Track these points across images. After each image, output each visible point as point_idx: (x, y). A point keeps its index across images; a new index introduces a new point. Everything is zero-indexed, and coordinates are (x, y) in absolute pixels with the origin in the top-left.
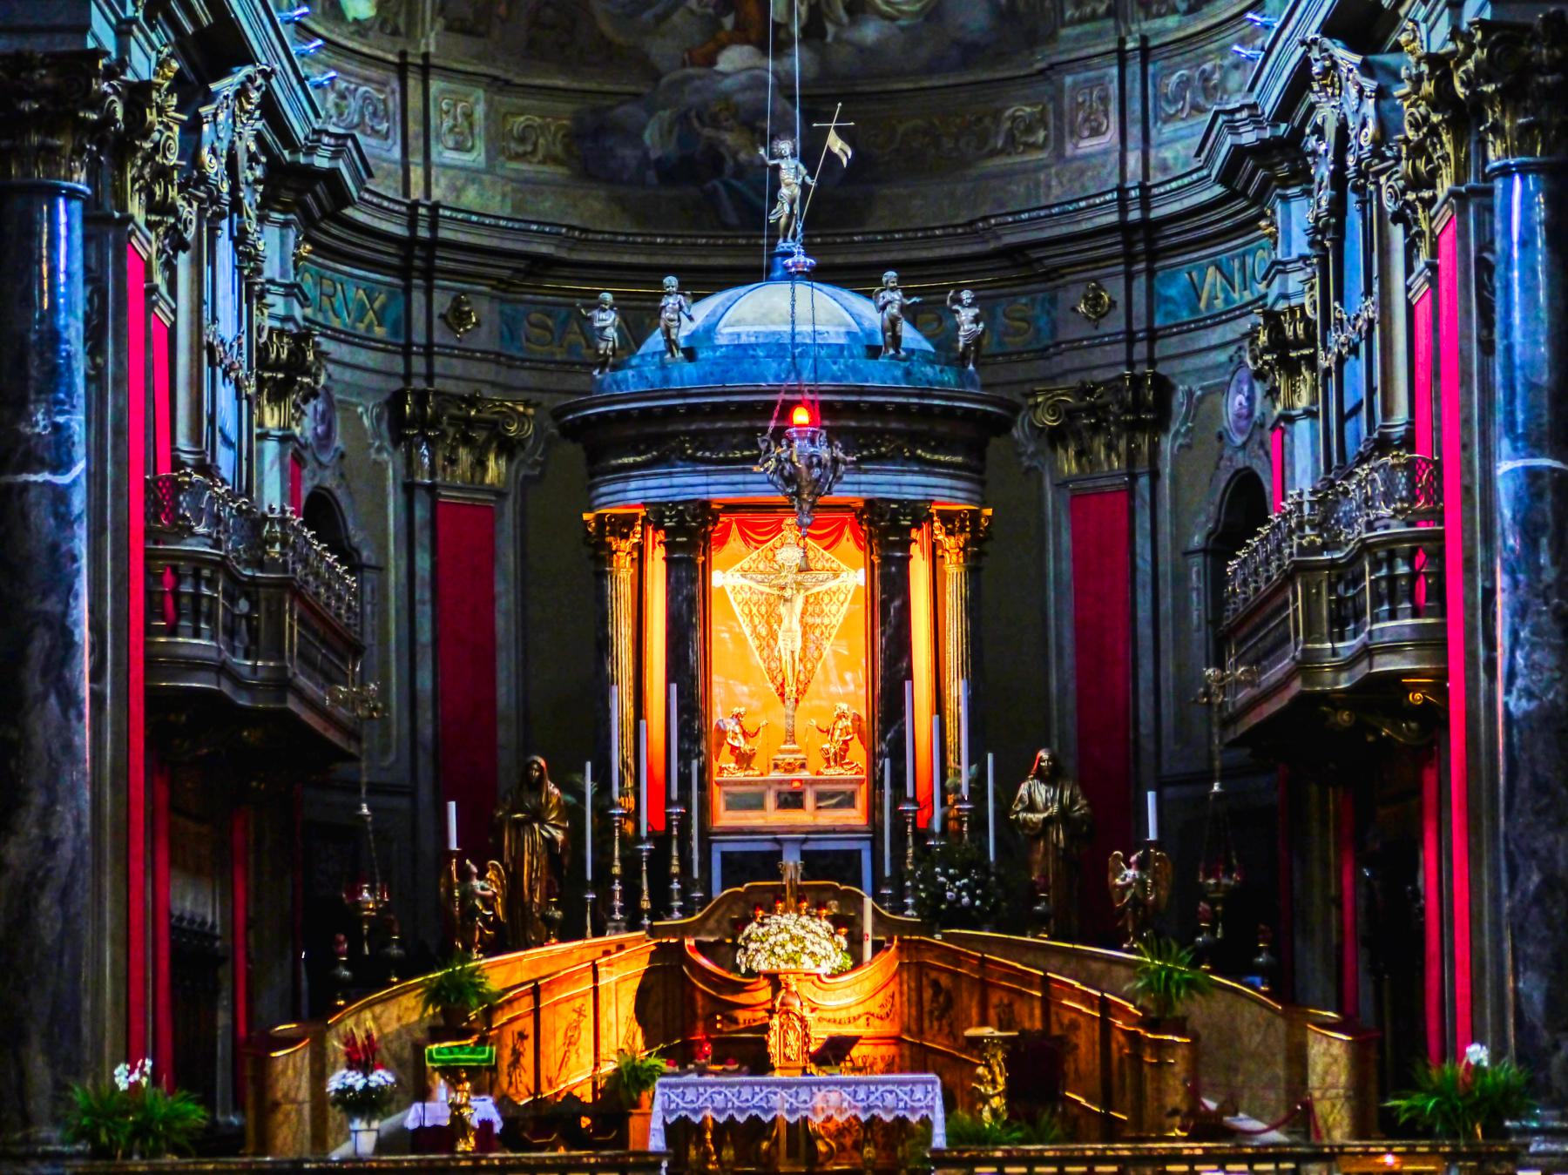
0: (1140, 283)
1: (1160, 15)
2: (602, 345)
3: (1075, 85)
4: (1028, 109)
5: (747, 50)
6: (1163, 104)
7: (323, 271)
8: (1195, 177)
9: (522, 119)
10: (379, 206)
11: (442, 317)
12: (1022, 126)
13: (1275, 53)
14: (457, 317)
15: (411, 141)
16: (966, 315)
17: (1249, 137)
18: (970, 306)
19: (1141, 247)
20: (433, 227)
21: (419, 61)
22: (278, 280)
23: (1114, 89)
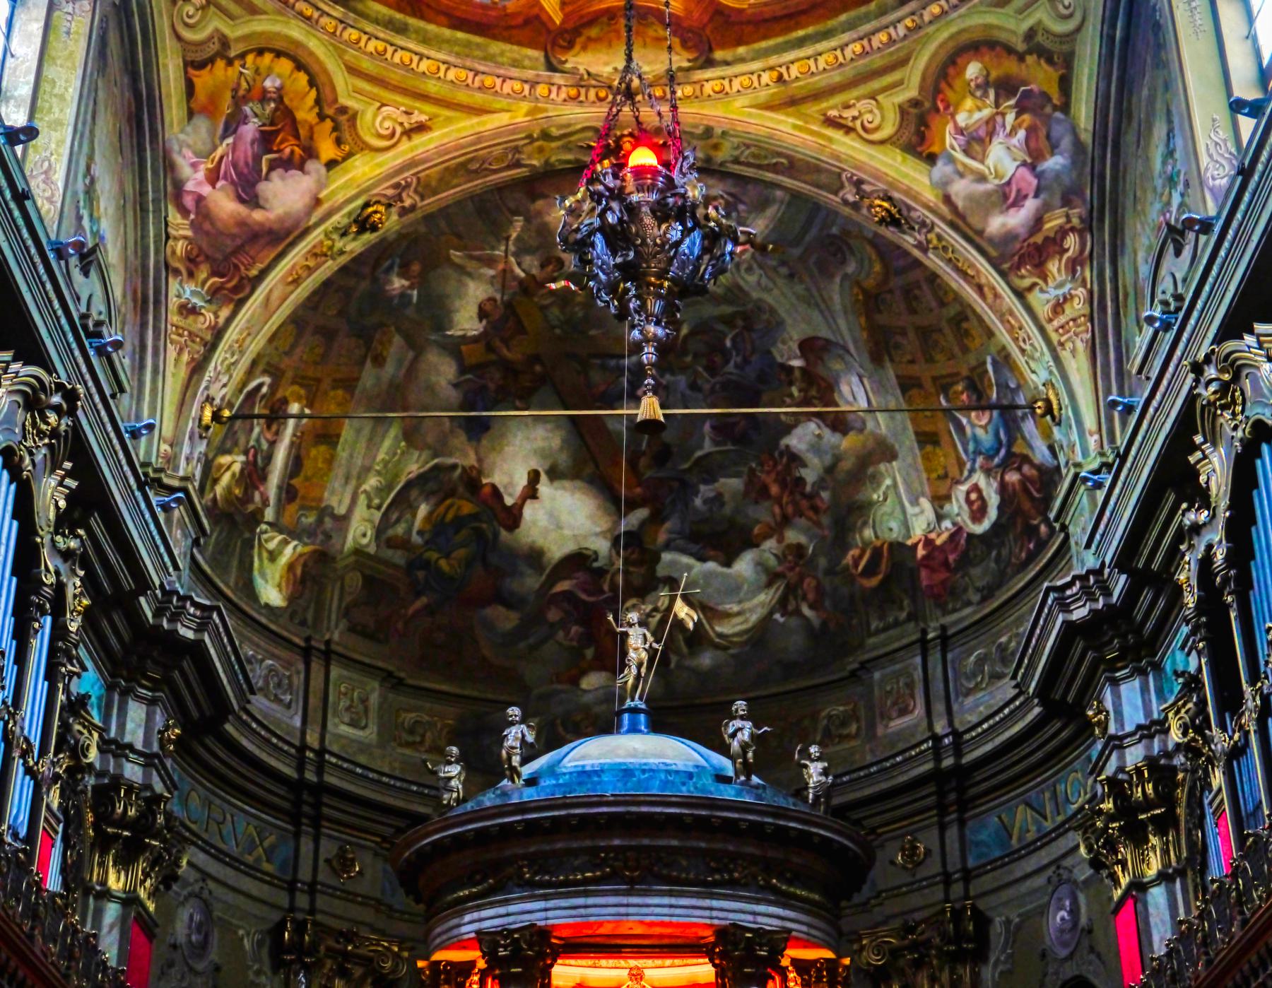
0: (952, 833)
1: (955, 610)
2: (446, 796)
3: (882, 680)
4: (841, 708)
6: (964, 682)
7: (212, 798)
8: (1006, 711)
9: (413, 715)
10: (268, 741)
11: (328, 861)
12: (837, 722)
13: (1130, 459)
14: (343, 863)
15: (310, 713)
18: (819, 759)
20: (320, 771)
21: (323, 647)
22: (139, 746)
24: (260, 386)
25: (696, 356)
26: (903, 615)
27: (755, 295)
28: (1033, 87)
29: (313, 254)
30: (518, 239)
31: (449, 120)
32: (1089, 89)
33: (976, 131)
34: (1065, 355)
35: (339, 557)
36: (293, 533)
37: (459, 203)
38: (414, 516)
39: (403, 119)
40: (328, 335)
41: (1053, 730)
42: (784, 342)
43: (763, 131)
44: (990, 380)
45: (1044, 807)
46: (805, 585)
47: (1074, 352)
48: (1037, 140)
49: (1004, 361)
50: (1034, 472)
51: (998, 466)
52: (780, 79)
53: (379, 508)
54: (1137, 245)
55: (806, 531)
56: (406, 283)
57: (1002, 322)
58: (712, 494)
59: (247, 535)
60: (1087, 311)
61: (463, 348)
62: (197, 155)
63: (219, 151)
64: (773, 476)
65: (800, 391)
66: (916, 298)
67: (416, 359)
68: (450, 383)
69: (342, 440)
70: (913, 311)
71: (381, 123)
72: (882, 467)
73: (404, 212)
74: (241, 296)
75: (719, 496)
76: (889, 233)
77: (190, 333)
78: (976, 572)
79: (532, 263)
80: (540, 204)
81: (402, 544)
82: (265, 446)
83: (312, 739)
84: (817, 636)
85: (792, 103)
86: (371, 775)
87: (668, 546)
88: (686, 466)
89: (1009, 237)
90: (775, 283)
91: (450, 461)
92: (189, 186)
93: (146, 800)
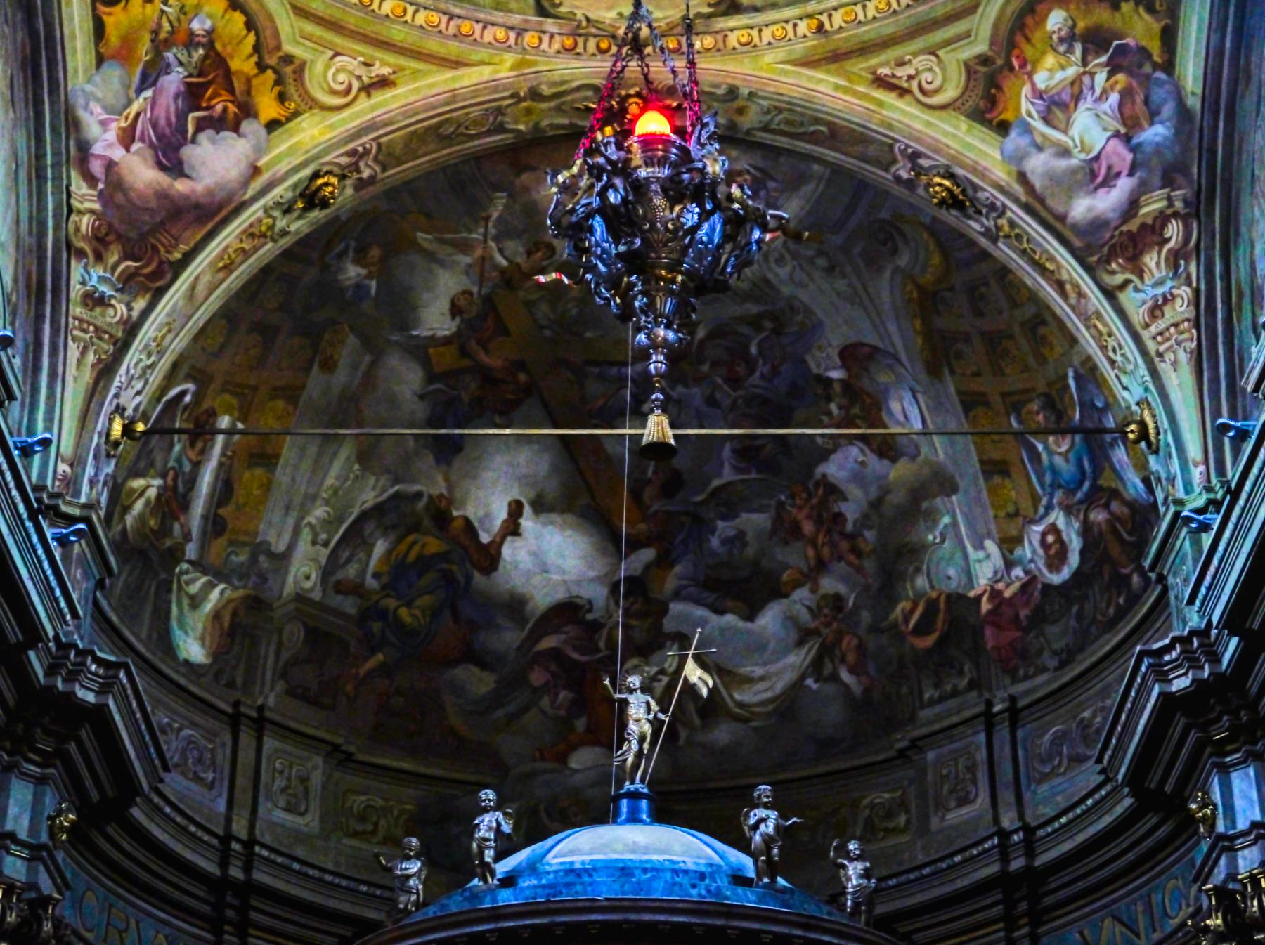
1: (1027, 677)
2: (403, 898)
4: (886, 796)
5: (597, 750)
6: (1037, 765)
7: (113, 898)
8: (1090, 802)
9: (363, 798)
10: (184, 829)
13: (1244, 496)
15: (238, 793)
16: (854, 870)
17: (1180, 683)
18: (859, 858)
19: (1023, 906)
20: (248, 868)
21: (254, 714)
22: (23, 835)
23: (982, 755)
24: (183, 394)
25: (714, 364)
26: (963, 683)
27: (786, 290)
28: (1129, 41)
29: (250, 234)
30: (500, 218)
31: (416, 74)
32: (1198, 40)
33: (1059, 94)
34: (1164, 368)
35: (276, 605)
36: (219, 574)
37: (429, 175)
38: (369, 556)
39: (361, 71)
40: (266, 332)
41: (1149, 825)
42: (820, 348)
43: (796, 93)
44: (1072, 397)
45: (1137, 921)
46: (844, 644)
47: (1175, 364)
48: (1134, 103)
49: (1090, 375)
50: (1126, 511)
51: (1081, 502)
52: (820, 28)
53: (326, 544)
54: (1254, 234)
55: (844, 579)
56: (363, 272)
57: (1088, 328)
58: (732, 533)
59: (163, 576)
60: (1191, 314)
61: (431, 351)
62: (106, 109)
63: (135, 107)
64: (806, 511)
65: (840, 408)
66: (982, 297)
67: (373, 364)
68: (415, 393)
69: (282, 461)
70: (979, 313)
71: (334, 75)
72: (938, 502)
73: (361, 185)
74: (159, 284)
75: (741, 535)
76: (951, 217)
77: (97, 329)
78: (1053, 630)
79: (516, 248)
80: (526, 177)
81: (355, 589)
82: (187, 467)
83: (240, 827)
84: (859, 706)
85: (834, 58)
86: (311, 872)
87: (677, 595)
88: (699, 498)
89: (1097, 224)
90: (812, 279)
91: (416, 488)
92: (97, 149)
93: (30, 902)
